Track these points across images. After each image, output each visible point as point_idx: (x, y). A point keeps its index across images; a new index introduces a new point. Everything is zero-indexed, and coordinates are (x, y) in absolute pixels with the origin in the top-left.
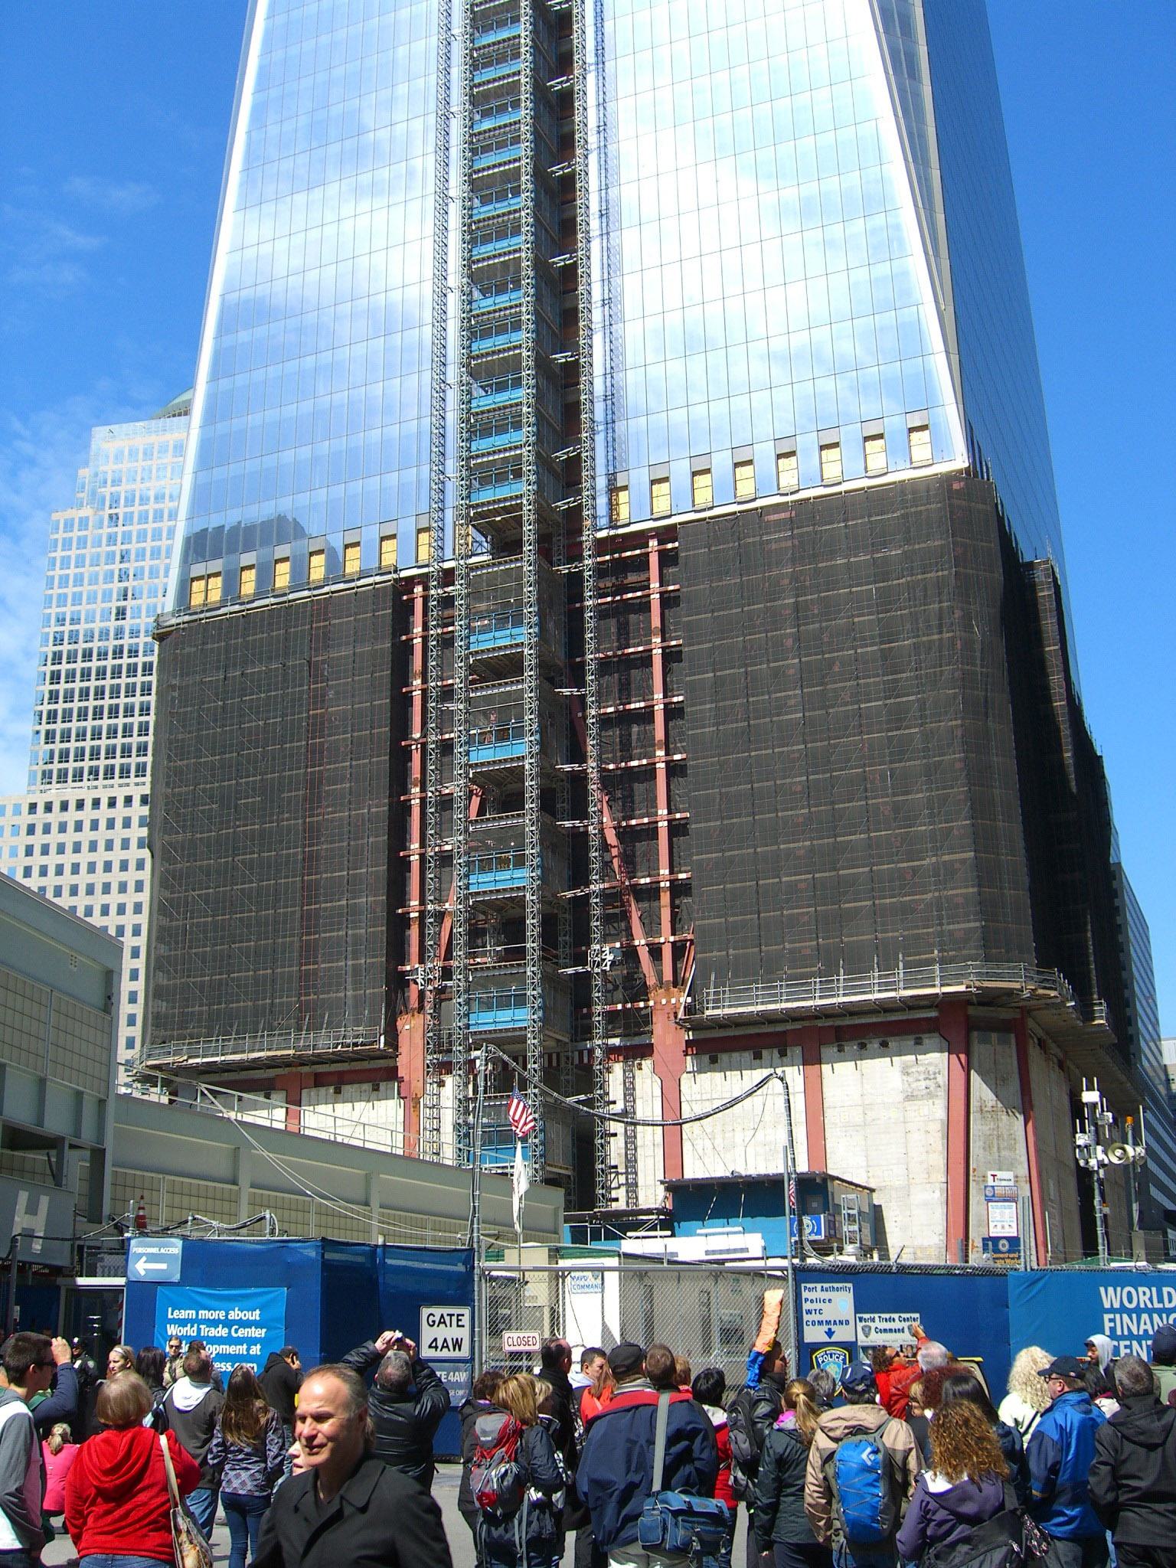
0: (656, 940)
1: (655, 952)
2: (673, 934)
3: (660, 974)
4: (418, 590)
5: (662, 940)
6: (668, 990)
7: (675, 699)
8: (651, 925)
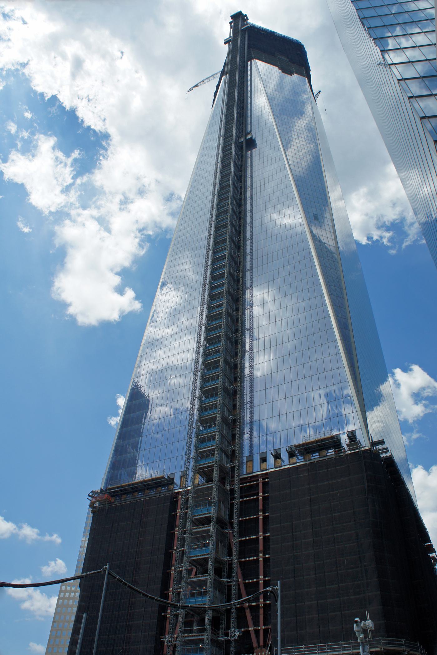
0: (257, 628)
1: (257, 632)
3: (258, 643)
5: (260, 628)
6: (261, 649)
8: (256, 624)
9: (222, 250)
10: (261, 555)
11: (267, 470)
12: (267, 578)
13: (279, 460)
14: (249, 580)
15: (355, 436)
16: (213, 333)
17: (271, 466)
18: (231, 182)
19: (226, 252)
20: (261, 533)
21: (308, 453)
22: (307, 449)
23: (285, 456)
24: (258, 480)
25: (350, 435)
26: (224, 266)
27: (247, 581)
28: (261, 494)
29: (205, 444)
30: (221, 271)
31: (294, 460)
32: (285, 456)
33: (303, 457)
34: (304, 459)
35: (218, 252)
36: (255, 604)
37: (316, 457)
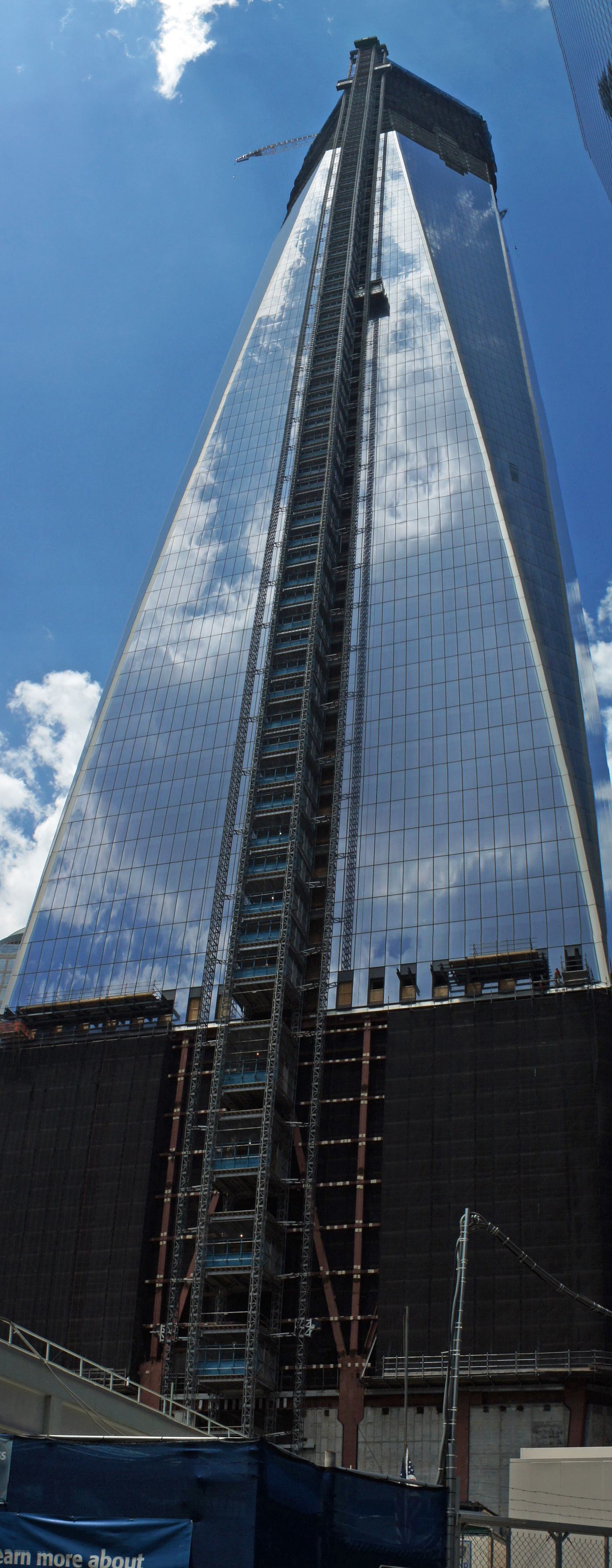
0: (347, 1318)
1: (346, 1326)
2: (361, 1314)
3: (347, 1344)
4: (186, 1042)
5: (352, 1318)
6: (353, 1356)
7: (375, 1139)
9: (309, 515)
10: (360, 1177)
11: (382, 1005)
12: (371, 1225)
13: (410, 989)
14: (332, 1224)
15: (580, 957)
16: (281, 693)
17: (391, 999)
18: (337, 371)
19: (321, 521)
20: (362, 1135)
21: (474, 980)
22: (471, 972)
23: (424, 977)
24: (363, 1025)
25: (572, 953)
26: (313, 550)
27: (328, 1228)
28: (367, 1054)
29: (256, 936)
30: (305, 561)
31: (443, 991)
32: (424, 977)
33: (463, 988)
34: (466, 991)
35: (300, 517)
36: (344, 1272)
37: (490, 990)
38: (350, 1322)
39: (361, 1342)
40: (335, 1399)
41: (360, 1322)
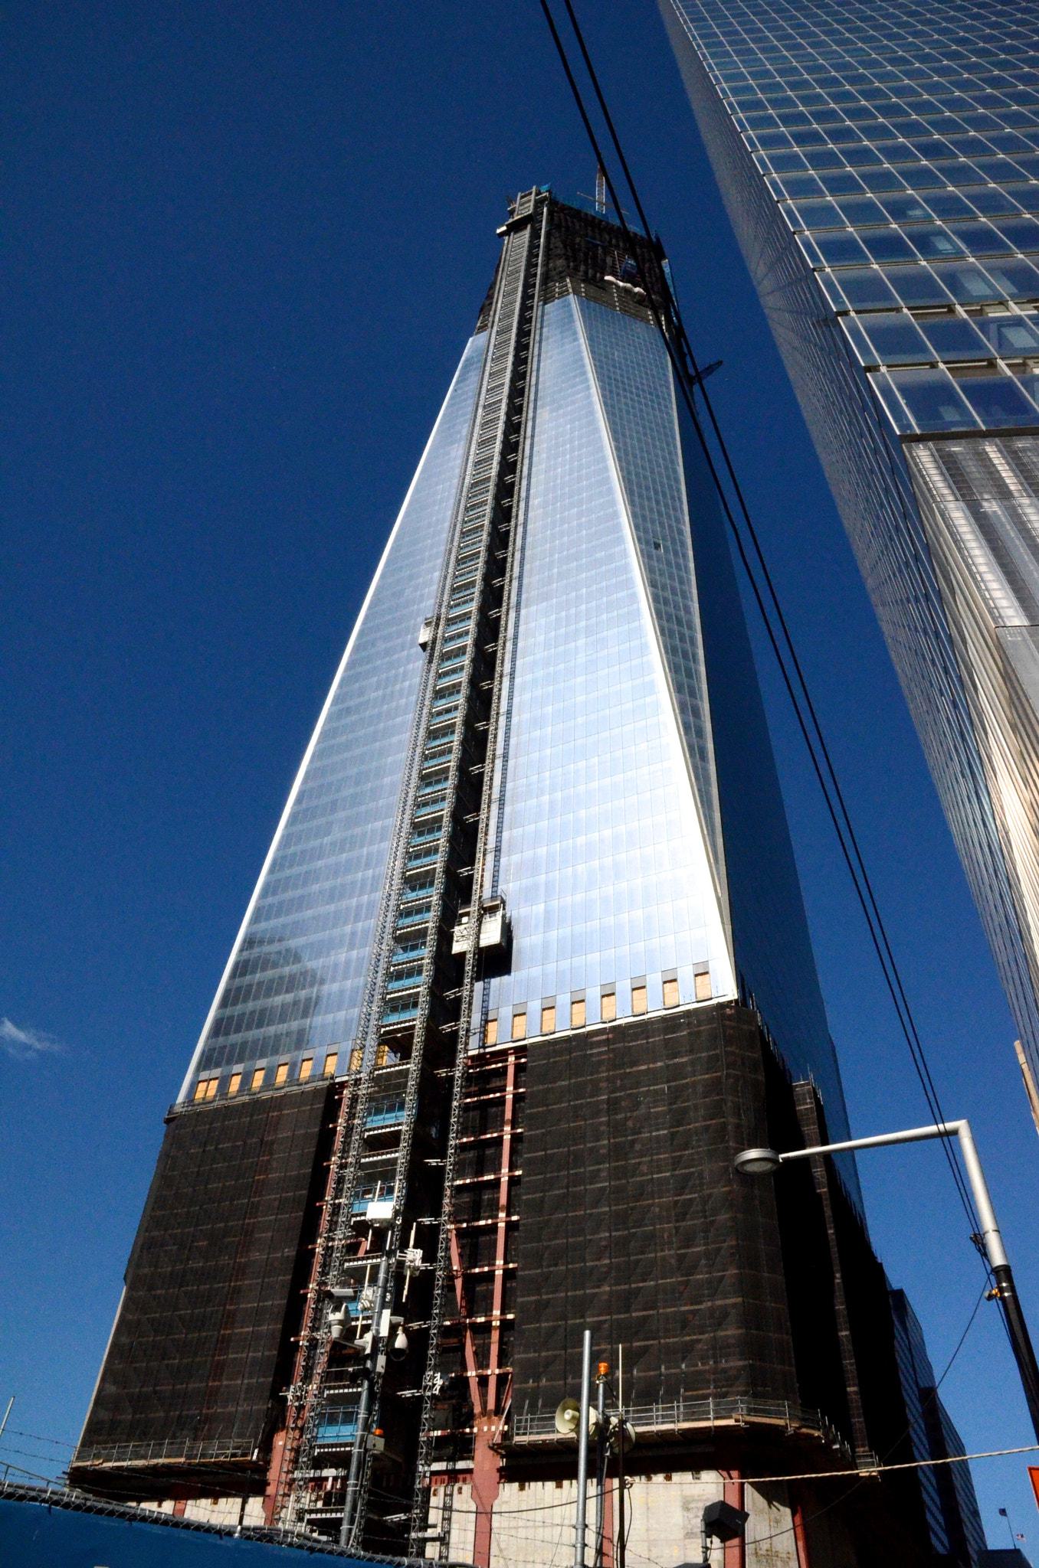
1: (483, 1381)
2: (499, 1367)
3: (484, 1404)
8: (482, 1361)
38: (487, 1376)
39: (498, 1400)
40: (470, 1471)
41: (498, 1376)
